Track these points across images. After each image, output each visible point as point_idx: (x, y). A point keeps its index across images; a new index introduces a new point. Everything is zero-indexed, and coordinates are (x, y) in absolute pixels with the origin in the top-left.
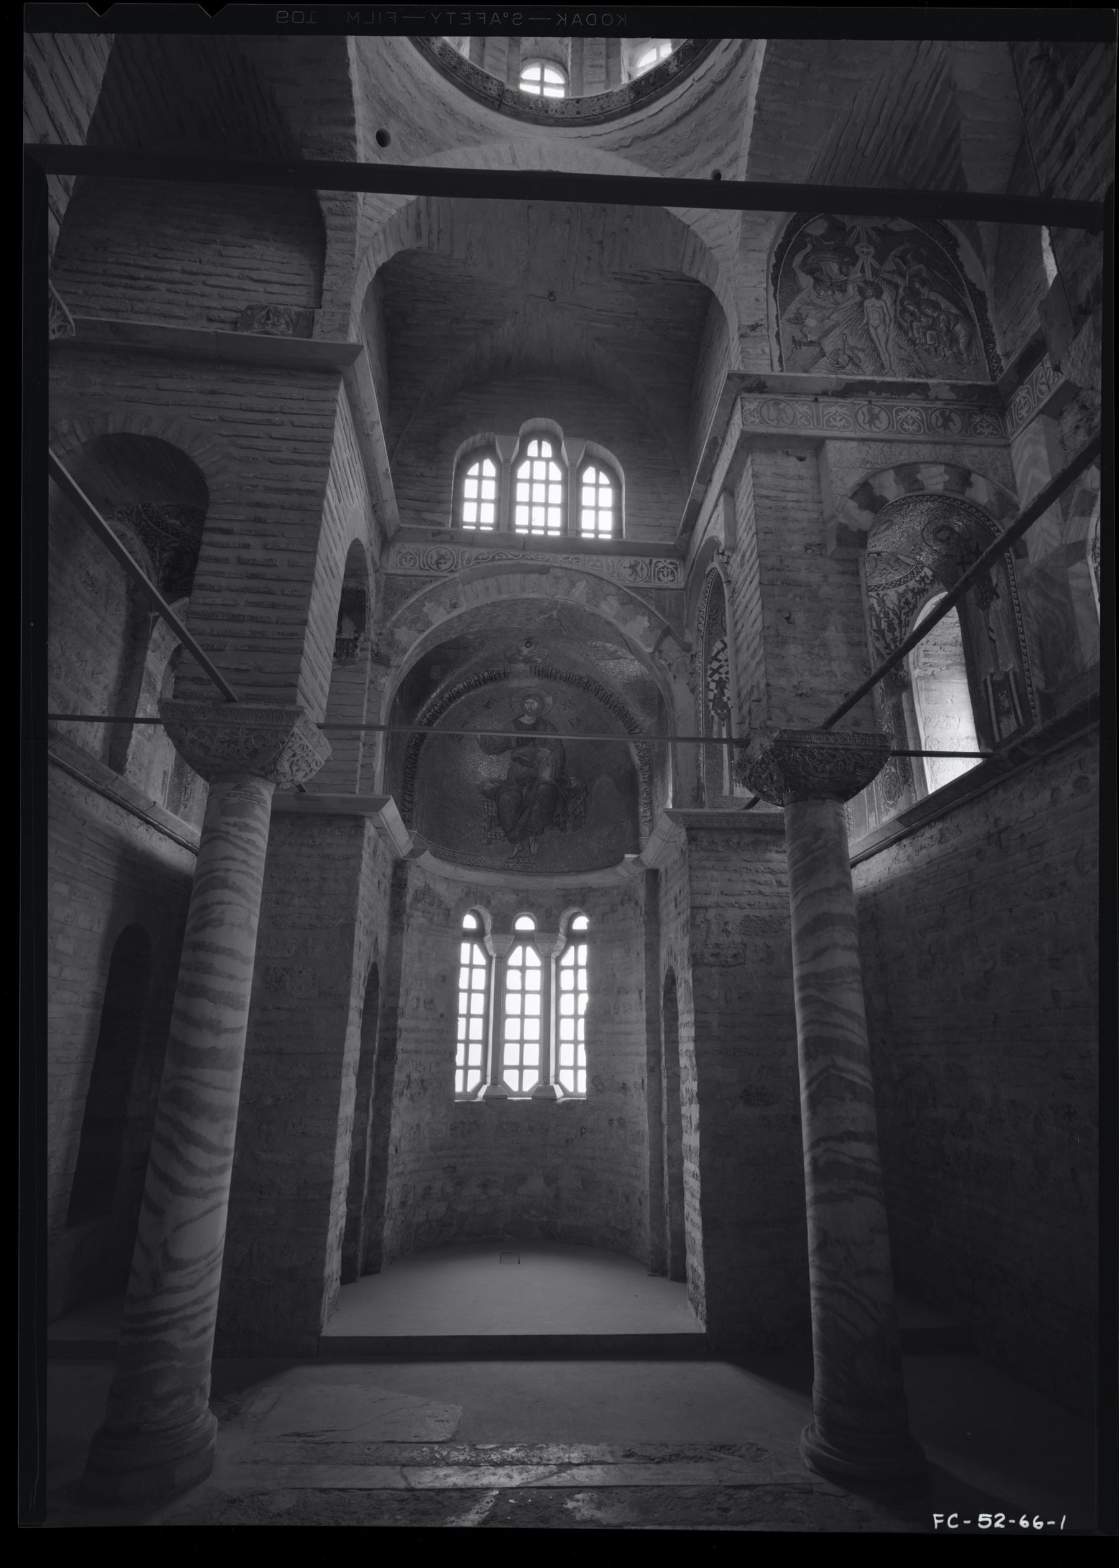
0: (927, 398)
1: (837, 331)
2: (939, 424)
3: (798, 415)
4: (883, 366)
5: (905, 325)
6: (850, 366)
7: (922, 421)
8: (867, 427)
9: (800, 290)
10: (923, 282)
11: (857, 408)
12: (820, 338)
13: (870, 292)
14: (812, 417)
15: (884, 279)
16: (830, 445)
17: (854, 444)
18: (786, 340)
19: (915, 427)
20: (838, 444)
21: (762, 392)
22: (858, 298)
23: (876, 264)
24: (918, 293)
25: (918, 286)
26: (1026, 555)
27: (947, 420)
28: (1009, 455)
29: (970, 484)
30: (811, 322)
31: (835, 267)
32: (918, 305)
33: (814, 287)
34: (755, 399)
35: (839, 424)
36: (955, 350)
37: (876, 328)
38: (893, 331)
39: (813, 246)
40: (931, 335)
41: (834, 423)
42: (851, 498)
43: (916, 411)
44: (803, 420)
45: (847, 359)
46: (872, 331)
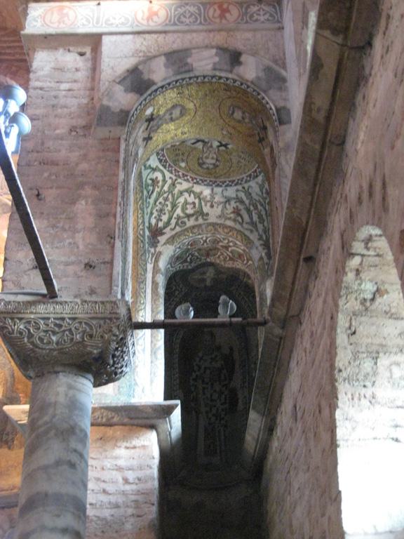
7: (200, 15)
14: (93, 19)
16: (105, 39)
17: (130, 37)
19: (192, 20)
20: (114, 38)
26: (289, 122)
28: (282, 36)
29: (239, 63)
42: (119, 83)
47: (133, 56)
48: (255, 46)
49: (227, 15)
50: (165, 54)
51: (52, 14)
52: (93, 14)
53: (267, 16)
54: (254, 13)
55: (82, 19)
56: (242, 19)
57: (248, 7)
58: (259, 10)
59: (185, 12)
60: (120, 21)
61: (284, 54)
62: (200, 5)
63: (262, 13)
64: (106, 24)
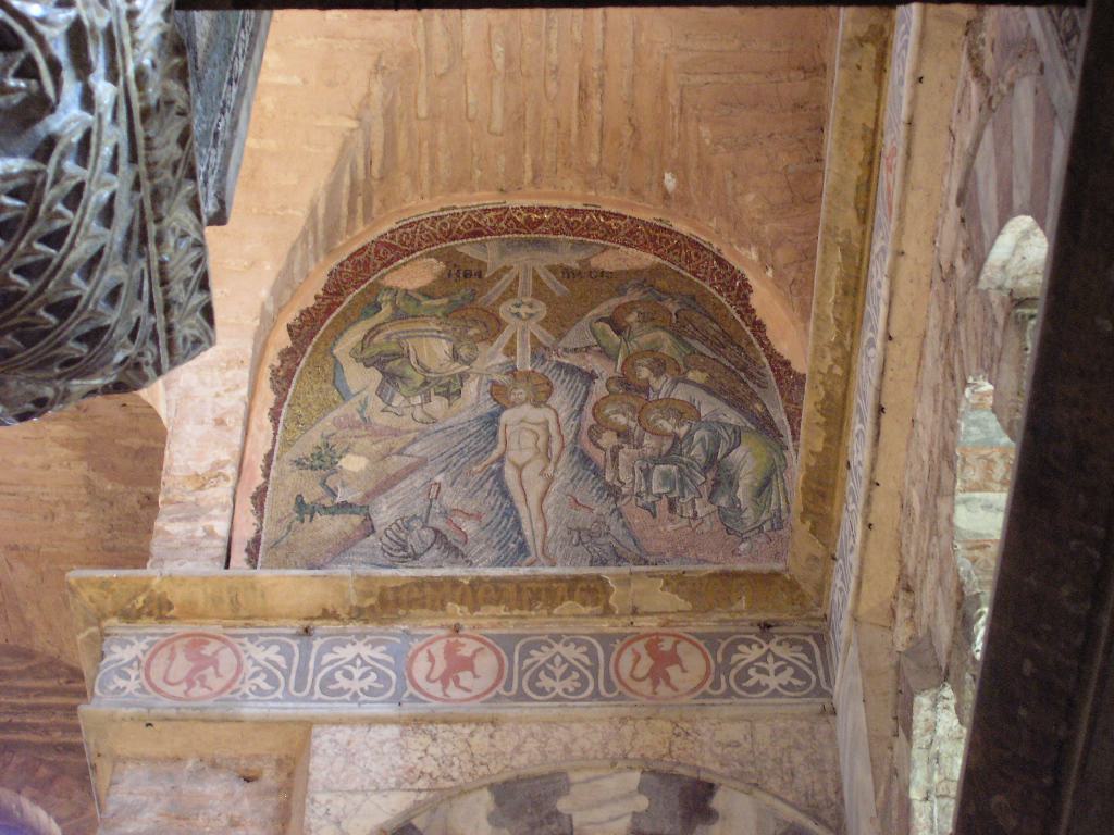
0: (607, 611)
1: (418, 480)
2: (642, 670)
3: (249, 668)
4: (523, 548)
5: (598, 456)
6: (434, 553)
7: (594, 671)
8: (435, 689)
9: (345, 395)
10: (660, 366)
11: (416, 644)
12: (367, 495)
13: (521, 393)
15: (560, 365)
16: (323, 740)
17: (392, 731)
18: (279, 503)
19: (571, 684)
20: (343, 734)
21: (162, 618)
22: (489, 406)
23: (544, 336)
24: (645, 389)
25: (645, 373)
27: (663, 662)
28: (832, 736)
29: (709, 816)
30: (353, 464)
31: (442, 348)
32: (640, 414)
33: (380, 392)
34: (140, 637)
35: (356, 685)
36: (723, 501)
37: (520, 469)
38: (563, 472)
39: (396, 308)
40: (665, 476)
41: (343, 683)
43: (579, 644)
44: (261, 681)
45: (428, 535)
46: (510, 474)
47: (398, 786)
48: (753, 763)
49: (673, 671)
50: (491, 787)
51: (172, 658)
52: (290, 664)
53: (785, 677)
54: (751, 665)
55: (255, 675)
56: (716, 685)
57: (731, 649)
58: (763, 658)
59: (551, 661)
60: (365, 684)
61: (839, 790)
62: (594, 641)
63: (771, 666)
64: (323, 688)
